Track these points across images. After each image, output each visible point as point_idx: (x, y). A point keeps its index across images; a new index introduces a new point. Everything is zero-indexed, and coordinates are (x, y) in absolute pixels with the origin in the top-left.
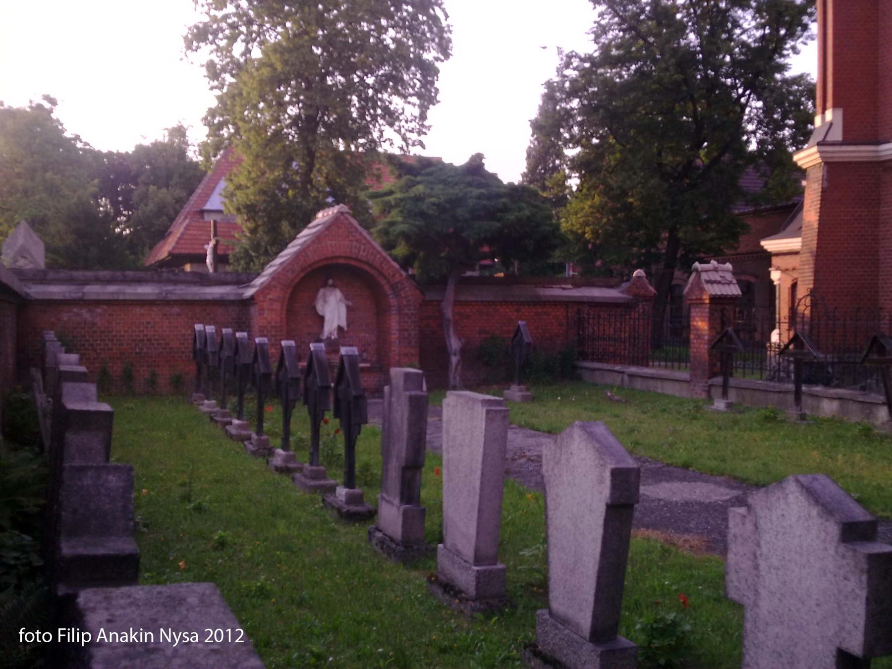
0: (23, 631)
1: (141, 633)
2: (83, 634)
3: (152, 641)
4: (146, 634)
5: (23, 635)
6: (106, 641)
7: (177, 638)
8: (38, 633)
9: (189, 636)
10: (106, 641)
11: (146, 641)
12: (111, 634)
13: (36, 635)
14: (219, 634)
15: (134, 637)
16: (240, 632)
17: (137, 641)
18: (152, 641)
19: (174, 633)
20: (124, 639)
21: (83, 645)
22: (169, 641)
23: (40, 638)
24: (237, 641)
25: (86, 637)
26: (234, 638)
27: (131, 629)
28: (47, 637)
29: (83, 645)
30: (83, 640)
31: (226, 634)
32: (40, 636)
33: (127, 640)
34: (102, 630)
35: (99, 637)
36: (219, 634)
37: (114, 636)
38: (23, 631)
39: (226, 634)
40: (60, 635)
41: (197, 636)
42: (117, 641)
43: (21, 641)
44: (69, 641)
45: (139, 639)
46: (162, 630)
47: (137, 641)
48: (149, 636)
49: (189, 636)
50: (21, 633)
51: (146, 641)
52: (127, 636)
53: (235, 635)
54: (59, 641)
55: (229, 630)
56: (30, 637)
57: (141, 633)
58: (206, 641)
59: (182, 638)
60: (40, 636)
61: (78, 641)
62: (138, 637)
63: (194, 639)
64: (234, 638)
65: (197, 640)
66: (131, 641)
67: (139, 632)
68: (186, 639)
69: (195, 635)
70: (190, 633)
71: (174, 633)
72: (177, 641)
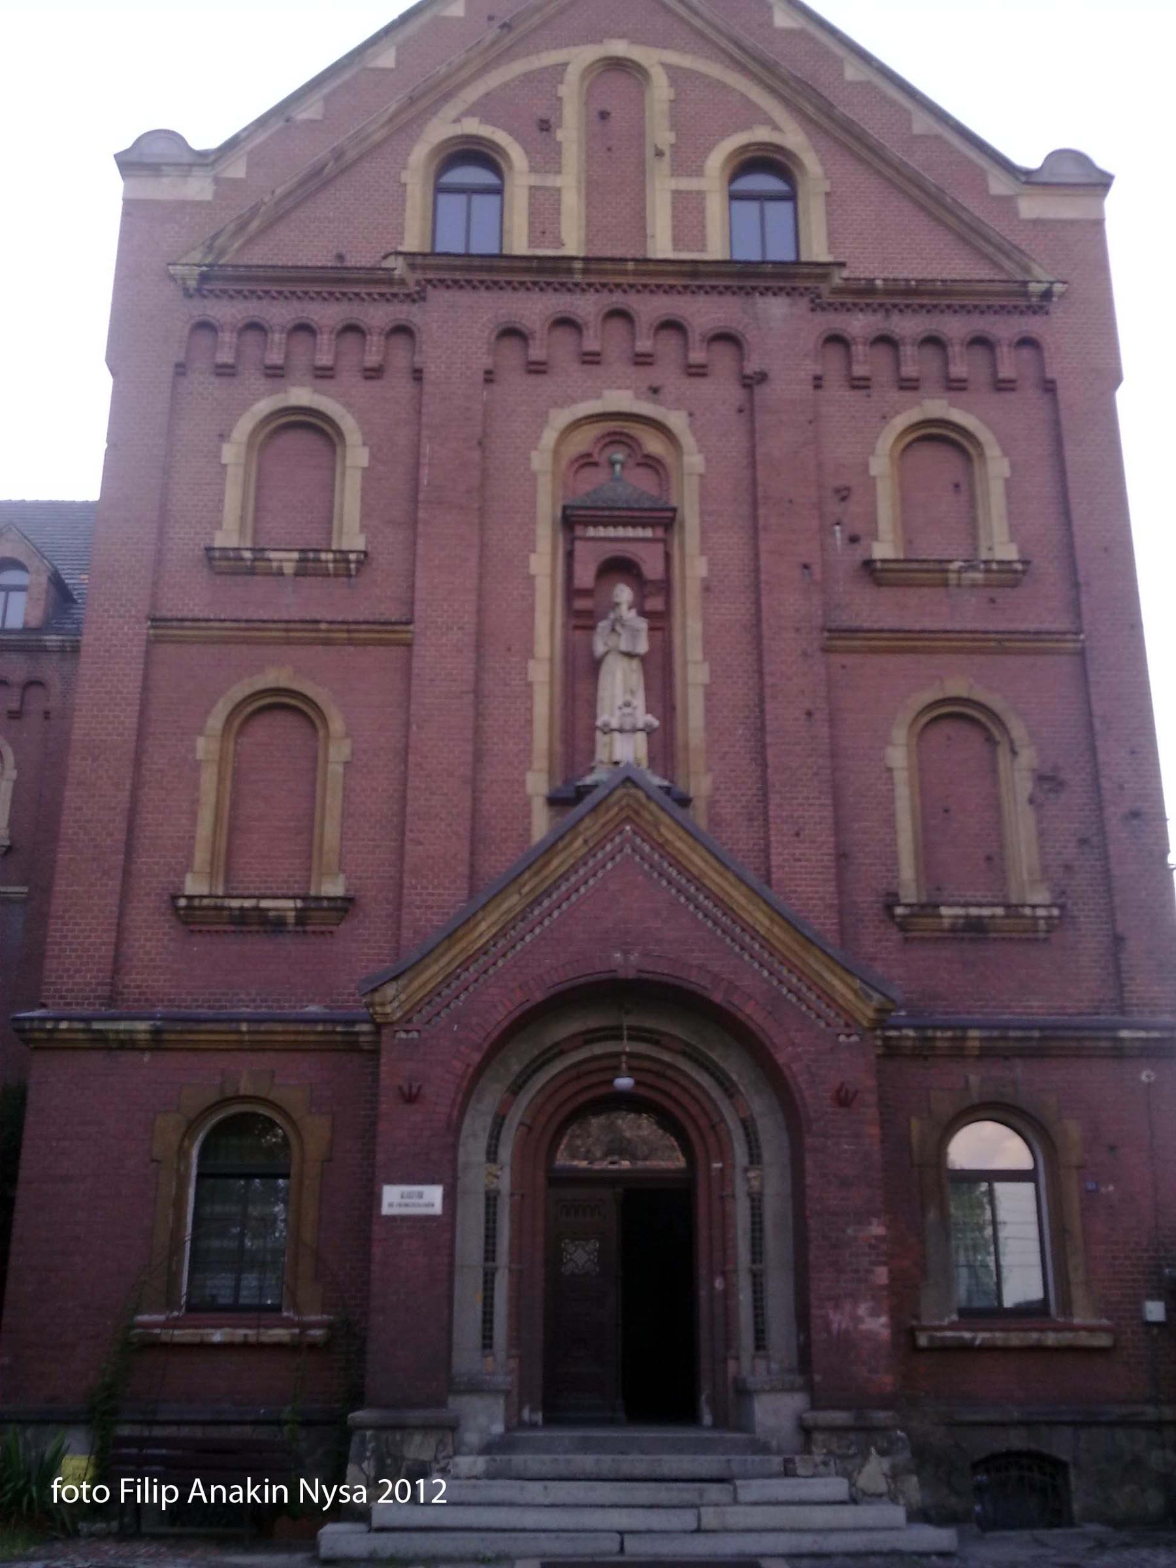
0: (59, 1483)
1: (267, 1487)
2: (164, 1489)
3: (286, 1501)
4: (275, 1489)
5: (59, 1491)
6: (205, 1501)
7: (330, 1495)
8: (85, 1486)
9: (352, 1492)
10: (205, 1501)
11: (274, 1501)
12: (213, 1489)
13: (80, 1490)
15: (253, 1493)
16: (440, 1485)
17: (259, 1501)
18: (286, 1501)
20: (236, 1497)
21: (164, 1508)
22: (316, 1500)
24: (435, 1501)
25: (170, 1494)
27: (249, 1479)
28: (101, 1494)
29: (164, 1508)
30: (164, 1499)
31: (415, 1488)
33: (241, 1500)
34: (197, 1481)
35: (193, 1494)
36: (403, 1487)
37: (218, 1492)
38: (59, 1483)
40: (123, 1491)
41: (364, 1493)
42: (224, 1501)
43: (55, 1501)
44: (139, 1501)
45: (262, 1498)
46: (302, 1481)
47: (259, 1501)
48: (280, 1492)
49: (352, 1492)
50: (55, 1486)
51: (274, 1501)
52: (241, 1493)
53: (432, 1490)
54: (123, 1501)
57: (267, 1487)
59: (338, 1494)
61: (155, 1501)
62: (260, 1493)
63: (360, 1497)
65: (364, 1500)
66: (249, 1501)
68: (345, 1498)
69: (361, 1490)
70: (352, 1486)
71: (324, 1487)
72: (330, 1500)
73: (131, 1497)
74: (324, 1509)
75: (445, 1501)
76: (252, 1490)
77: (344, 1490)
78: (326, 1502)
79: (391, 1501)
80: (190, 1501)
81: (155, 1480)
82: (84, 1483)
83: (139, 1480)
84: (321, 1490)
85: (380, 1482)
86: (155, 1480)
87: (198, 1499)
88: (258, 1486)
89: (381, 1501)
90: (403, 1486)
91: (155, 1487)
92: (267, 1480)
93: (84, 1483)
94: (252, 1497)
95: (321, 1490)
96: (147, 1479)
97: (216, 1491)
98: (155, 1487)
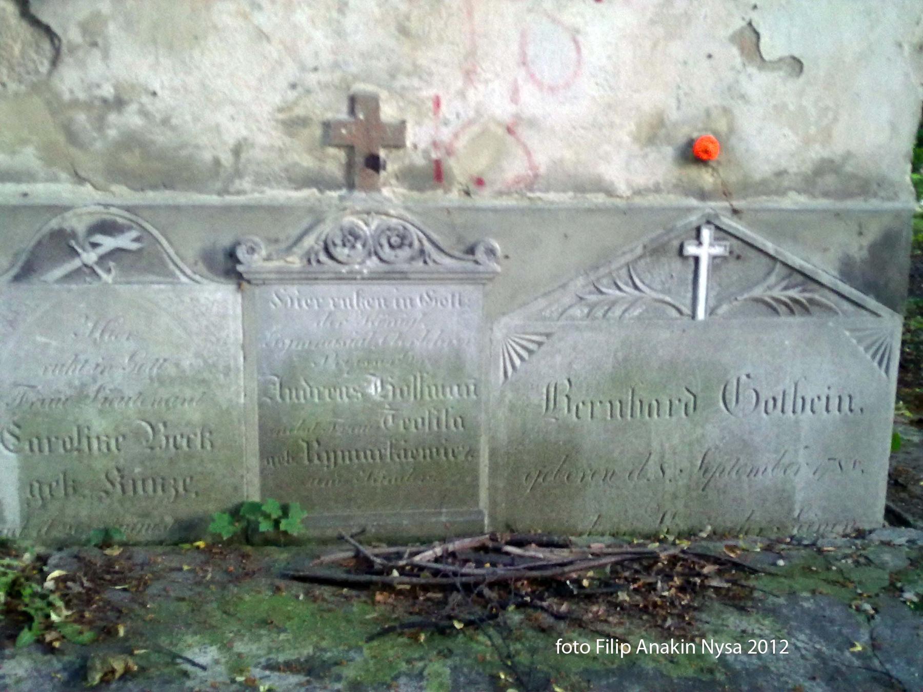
3: (694, 652)
4: (687, 645)
5: (561, 646)
6: (646, 653)
11: (687, 652)
12: (651, 645)
18: (694, 652)
19: (716, 644)
20: (665, 650)
21: (622, 657)
22: (712, 652)
24: (782, 652)
26: (778, 650)
28: (585, 648)
29: (622, 657)
30: (622, 652)
31: (770, 645)
32: (578, 647)
33: (667, 652)
35: (639, 648)
37: (654, 648)
39: (770, 645)
40: (598, 647)
44: (607, 652)
45: (680, 652)
48: (691, 647)
50: (558, 644)
51: (687, 652)
52: (667, 648)
53: (780, 646)
55: (774, 641)
58: (750, 652)
59: (725, 649)
60: (578, 647)
61: (617, 652)
63: (737, 650)
65: (740, 652)
66: (672, 652)
67: (680, 643)
68: (729, 651)
69: (738, 646)
71: (716, 644)
72: (720, 652)
73: (603, 651)
77: (728, 646)
80: (637, 652)
90: (763, 644)
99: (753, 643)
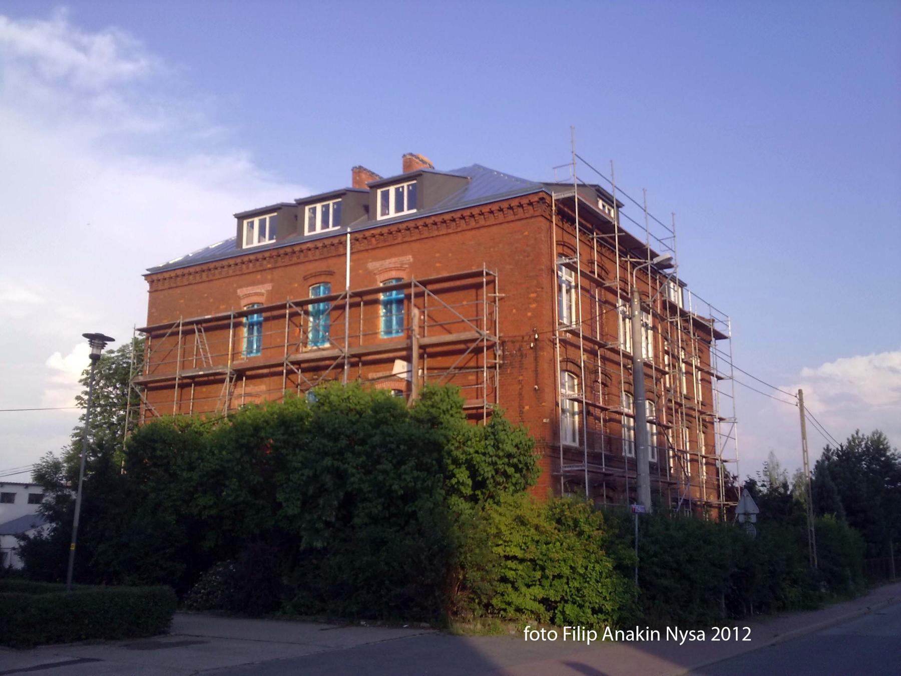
1: (647, 632)
2: (589, 633)
3: (659, 639)
4: (652, 633)
5: (529, 634)
6: (612, 640)
8: (543, 631)
9: (696, 634)
10: (612, 640)
11: (652, 639)
12: (617, 633)
13: (541, 633)
14: (726, 631)
15: (640, 635)
16: (747, 630)
17: (643, 640)
18: (659, 639)
19: (680, 631)
20: (630, 637)
21: (588, 643)
22: (676, 639)
23: (546, 636)
24: (744, 639)
25: (592, 635)
26: (741, 637)
27: (637, 627)
28: (552, 635)
29: (588, 643)
31: (733, 632)
33: (633, 639)
35: (605, 635)
36: (726, 631)
37: (620, 634)
39: (733, 632)
40: (565, 634)
41: (704, 635)
42: (623, 640)
43: (526, 639)
44: (574, 639)
46: (668, 628)
47: (643, 640)
48: (655, 635)
49: (696, 634)
50: (526, 631)
51: (652, 639)
52: (633, 635)
53: (742, 633)
55: (736, 628)
56: (535, 635)
57: (647, 632)
58: (713, 639)
60: (546, 634)
61: (583, 639)
62: (644, 635)
63: (701, 637)
64: (741, 635)
65: (704, 639)
66: (637, 639)
68: (692, 638)
69: (701, 633)
71: (680, 631)
72: (684, 639)
74: (681, 644)
75: (750, 640)
76: (639, 633)
78: (682, 640)
79: (719, 640)
81: (584, 628)
82: (543, 629)
83: (574, 628)
84: (678, 632)
85: (713, 628)
86: (584, 628)
87: (608, 639)
88: (643, 631)
89: (713, 639)
90: (726, 631)
91: (584, 631)
92: (648, 628)
93: (543, 629)
94: (639, 637)
95: (678, 632)
96: (579, 627)
97: (619, 633)
98: (584, 631)
99: (716, 630)
